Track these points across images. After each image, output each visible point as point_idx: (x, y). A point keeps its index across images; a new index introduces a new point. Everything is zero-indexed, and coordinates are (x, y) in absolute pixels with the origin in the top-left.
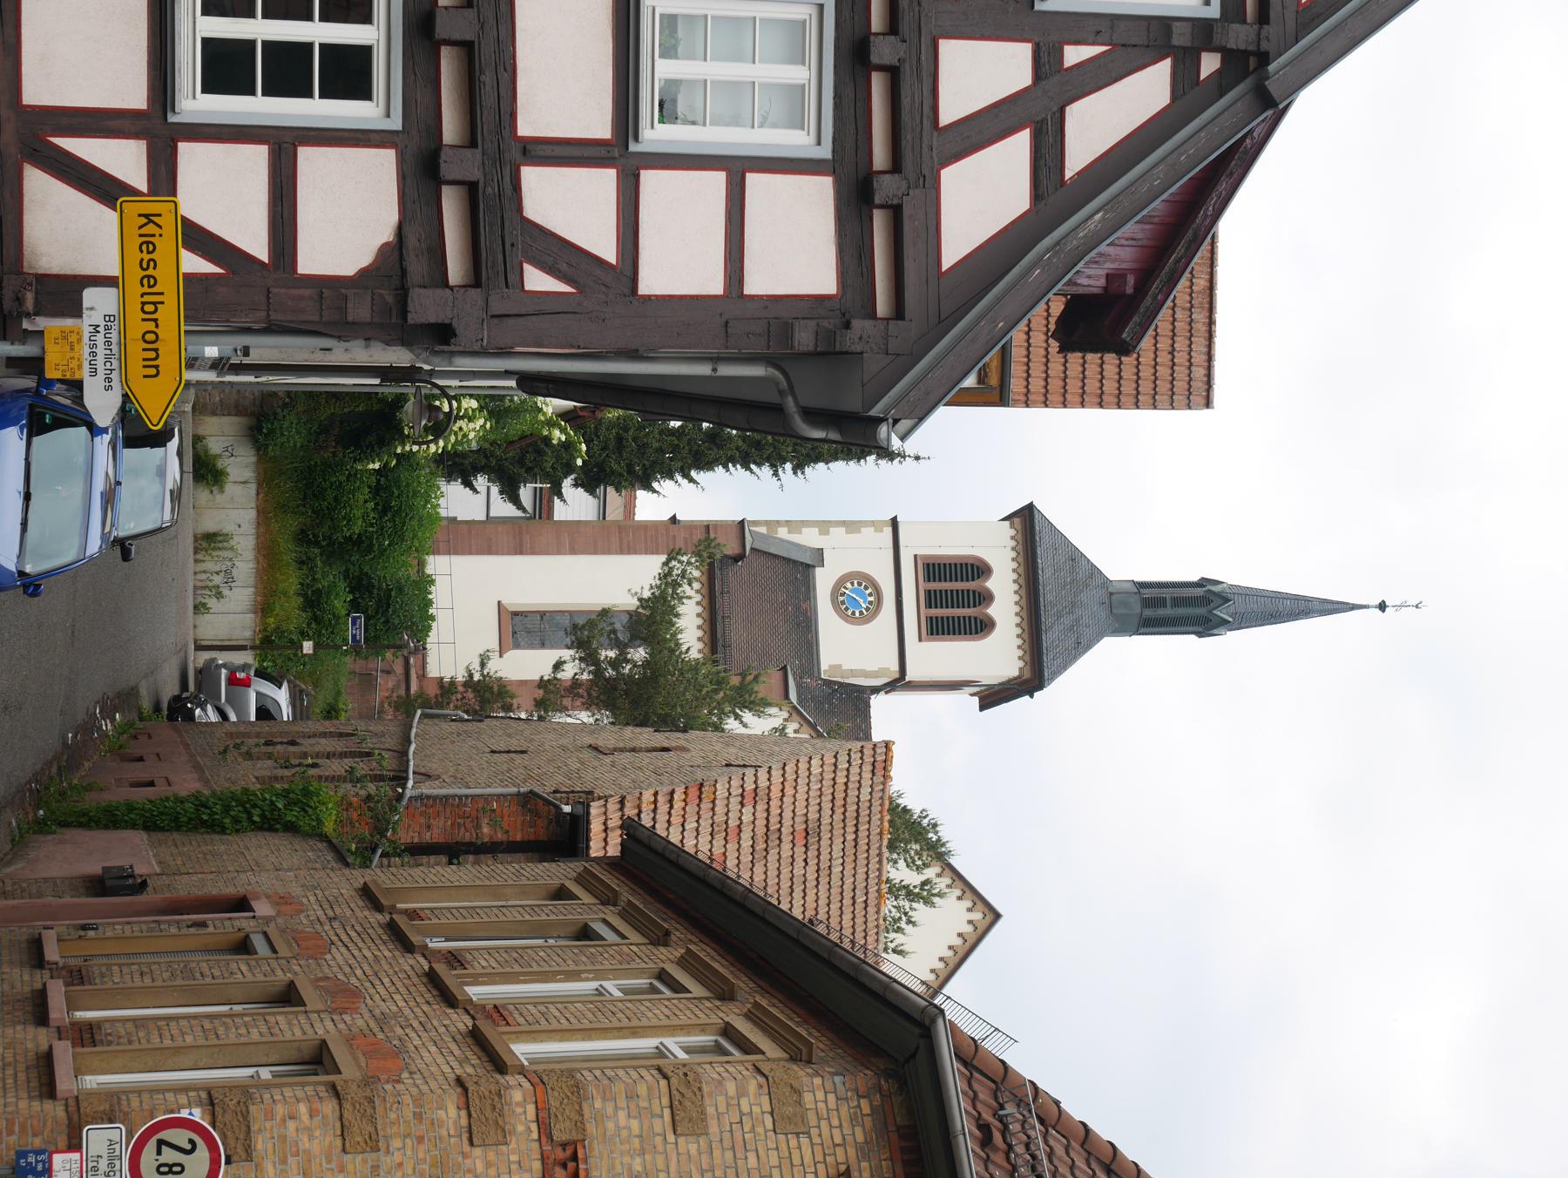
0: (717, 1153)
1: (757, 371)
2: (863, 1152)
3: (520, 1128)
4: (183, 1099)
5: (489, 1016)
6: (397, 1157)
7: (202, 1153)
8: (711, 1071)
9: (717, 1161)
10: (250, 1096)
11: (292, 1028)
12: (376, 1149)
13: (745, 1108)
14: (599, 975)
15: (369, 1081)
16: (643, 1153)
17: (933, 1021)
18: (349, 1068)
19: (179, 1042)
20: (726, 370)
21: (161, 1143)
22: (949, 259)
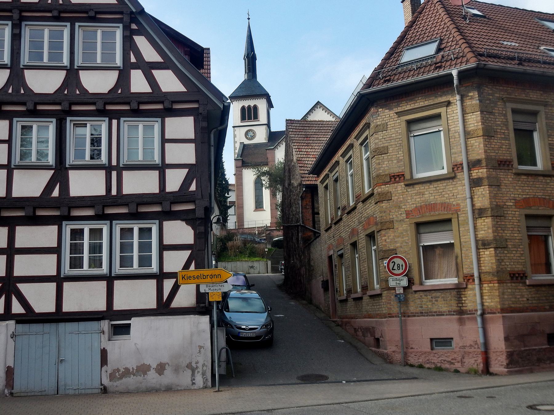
0: (392, 144)
1: (212, 136)
2: (390, 109)
3: (387, 189)
4: (382, 265)
5: (359, 199)
6: (394, 216)
7: (395, 260)
8: (372, 146)
9: (394, 143)
10: (381, 250)
11: (362, 243)
12: (393, 221)
13: (381, 137)
14: (347, 175)
15: (376, 224)
16: (392, 161)
17: (360, 94)
18: (374, 229)
19: (367, 268)
20: (212, 143)
21: (393, 269)
22: (183, 89)
